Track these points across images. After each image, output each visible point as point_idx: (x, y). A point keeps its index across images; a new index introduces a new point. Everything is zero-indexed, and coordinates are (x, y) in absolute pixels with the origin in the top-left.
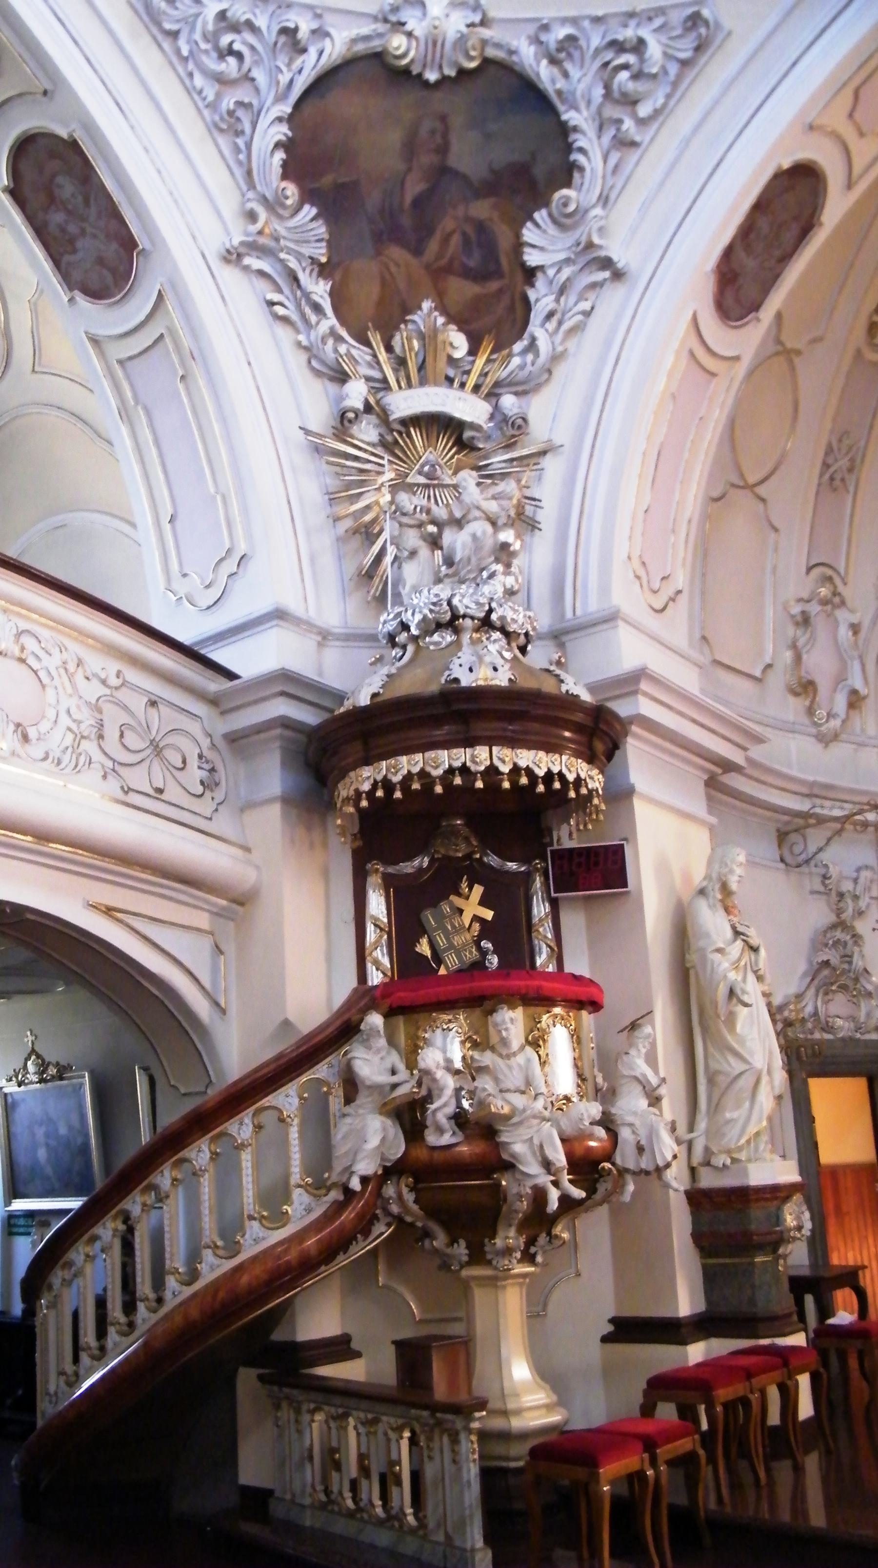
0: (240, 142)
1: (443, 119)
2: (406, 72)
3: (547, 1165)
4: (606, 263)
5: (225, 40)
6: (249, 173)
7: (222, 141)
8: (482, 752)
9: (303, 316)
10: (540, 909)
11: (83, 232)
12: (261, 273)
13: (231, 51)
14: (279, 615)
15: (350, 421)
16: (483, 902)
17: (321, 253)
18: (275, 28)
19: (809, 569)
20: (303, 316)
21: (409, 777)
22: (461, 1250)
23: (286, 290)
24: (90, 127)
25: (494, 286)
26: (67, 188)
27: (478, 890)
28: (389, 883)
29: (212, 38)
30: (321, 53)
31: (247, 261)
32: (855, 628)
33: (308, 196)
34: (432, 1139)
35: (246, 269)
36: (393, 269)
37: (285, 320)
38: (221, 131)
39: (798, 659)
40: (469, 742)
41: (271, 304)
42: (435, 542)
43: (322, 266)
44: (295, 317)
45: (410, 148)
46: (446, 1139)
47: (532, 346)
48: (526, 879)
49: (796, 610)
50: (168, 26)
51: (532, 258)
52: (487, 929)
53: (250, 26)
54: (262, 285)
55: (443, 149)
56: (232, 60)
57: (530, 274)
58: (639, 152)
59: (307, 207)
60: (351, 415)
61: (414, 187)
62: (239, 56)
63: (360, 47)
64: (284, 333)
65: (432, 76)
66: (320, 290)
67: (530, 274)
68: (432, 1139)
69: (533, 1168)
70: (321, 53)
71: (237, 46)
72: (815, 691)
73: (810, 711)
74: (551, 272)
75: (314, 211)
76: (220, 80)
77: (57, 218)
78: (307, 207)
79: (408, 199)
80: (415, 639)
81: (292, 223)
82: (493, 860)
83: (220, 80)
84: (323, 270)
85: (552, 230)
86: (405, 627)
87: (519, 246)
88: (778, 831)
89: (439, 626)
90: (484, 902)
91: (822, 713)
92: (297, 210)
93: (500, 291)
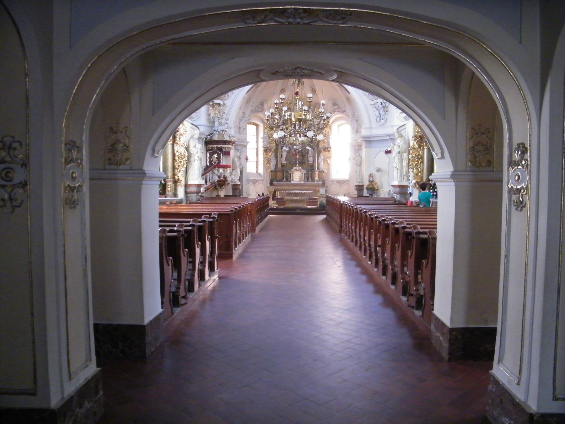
3: (230, 181)
10: (221, 157)
21: (220, 147)
22: (219, 188)
27: (216, 154)
28: (210, 153)
32: (245, 120)
34: (221, 178)
39: (239, 125)
40: (226, 145)
42: (219, 120)
46: (223, 179)
47: (228, 95)
48: (220, 154)
49: (240, 118)
52: (217, 158)
68: (221, 178)
69: (229, 181)
73: (239, 131)
86: (217, 130)
89: (221, 131)
90: (217, 155)
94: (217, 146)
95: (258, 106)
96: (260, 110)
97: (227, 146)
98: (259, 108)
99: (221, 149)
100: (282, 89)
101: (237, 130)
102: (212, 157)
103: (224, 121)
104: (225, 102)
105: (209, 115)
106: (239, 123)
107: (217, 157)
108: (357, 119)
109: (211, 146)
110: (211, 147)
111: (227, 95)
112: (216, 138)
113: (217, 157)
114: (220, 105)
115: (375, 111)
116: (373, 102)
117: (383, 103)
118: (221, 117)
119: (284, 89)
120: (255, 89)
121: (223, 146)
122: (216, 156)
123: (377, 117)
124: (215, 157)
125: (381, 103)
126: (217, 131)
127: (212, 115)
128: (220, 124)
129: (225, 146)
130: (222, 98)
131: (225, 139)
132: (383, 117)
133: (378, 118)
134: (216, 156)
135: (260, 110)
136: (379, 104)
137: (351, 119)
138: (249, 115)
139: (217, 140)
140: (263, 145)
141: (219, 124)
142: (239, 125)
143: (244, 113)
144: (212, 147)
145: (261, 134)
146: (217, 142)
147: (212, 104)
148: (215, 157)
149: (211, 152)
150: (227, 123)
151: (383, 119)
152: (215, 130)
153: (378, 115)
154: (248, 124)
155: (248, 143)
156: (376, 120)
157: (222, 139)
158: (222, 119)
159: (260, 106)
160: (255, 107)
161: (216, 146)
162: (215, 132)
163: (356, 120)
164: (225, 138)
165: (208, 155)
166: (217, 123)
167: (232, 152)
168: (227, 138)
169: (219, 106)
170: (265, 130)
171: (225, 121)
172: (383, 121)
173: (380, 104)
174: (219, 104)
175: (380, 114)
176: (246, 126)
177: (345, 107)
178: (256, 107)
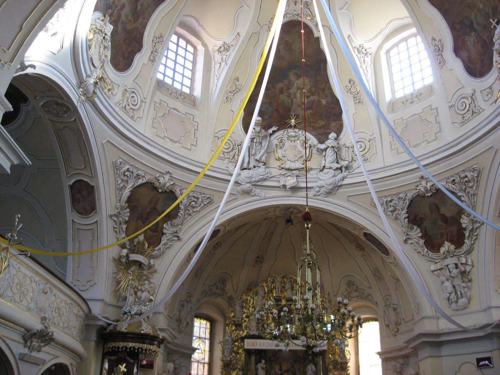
0: (121, 192)
1: (159, 198)
2: (155, 188)
4: (178, 237)
5: (126, 173)
6: (120, 200)
7: (117, 191)
8: (145, 345)
9: (120, 232)
10: (135, 370)
11: (83, 201)
12: (115, 221)
13: (127, 176)
14: (102, 300)
15: (122, 258)
16: (122, 366)
17: (127, 219)
18: (136, 173)
19: (187, 294)
20: (120, 232)
21: (131, 347)
23: (118, 225)
24: (98, 187)
25: (156, 234)
26: (85, 193)
27: (124, 365)
28: (110, 362)
29: (124, 172)
30: (143, 180)
31: (113, 218)
32: (191, 308)
33: (128, 207)
35: (113, 219)
36: (138, 225)
37: (116, 232)
38: (118, 189)
40: (144, 343)
41: (114, 228)
42: (136, 293)
43: (126, 221)
44: (118, 232)
45: (150, 202)
48: (133, 365)
50: (117, 168)
51: (165, 231)
53: (132, 172)
54: (115, 224)
55: (156, 204)
56: (126, 177)
57: (163, 234)
58: (191, 217)
59: (128, 209)
60: (123, 257)
61: (148, 210)
62: (128, 177)
63: (149, 181)
64: (114, 233)
65: (160, 191)
66: (124, 227)
67: (163, 234)
70: (143, 180)
71: (128, 175)
72: (181, 322)
73: (179, 326)
74: (167, 235)
75: (129, 211)
76: (123, 180)
77: (79, 196)
78: (128, 209)
79: (146, 212)
80: (131, 315)
81: (124, 212)
82: (128, 358)
83: (123, 180)
84: (126, 222)
85: (170, 225)
86: (130, 312)
87: (163, 227)
88: (168, 352)
89: (137, 314)
91: (181, 326)
92: (126, 209)
93: (156, 235)
94: (125, 344)
95: (215, 284)
96: (219, 291)
97: (146, 346)
98: (217, 288)
99: (134, 354)
100: (258, 257)
101: (175, 325)
102: (115, 369)
103: (144, 295)
104: (152, 261)
105: (118, 283)
106: (180, 311)
107: (125, 370)
108: (396, 306)
109: (113, 344)
110: (113, 347)
111: (157, 248)
112: (123, 327)
113: (125, 370)
114: (142, 266)
115: (443, 283)
116: (433, 267)
117: (459, 264)
118: (140, 287)
119: (262, 258)
120: (212, 251)
121: (137, 345)
122: (123, 368)
123: (450, 293)
124: (122, 370)
125: (456, 264)
126: (129, 314)
127: (123, 284)
128: (139, 301)
129: (141, 345)
130: (147, 253)
131: (142, 332)
132: (463, 291)
133: (453, 294)
134: (123, 368)
135: (219, 291)
136: (452, 266)
137: (384, 309)
138: (199, 300)
139: (126, 331)
140: (221, 356)
141: (135, 302)
142: (180, 314)
143: (190, 295)
144: (115, 347)
145: (219, 337)
146: (124, 336)
147: (126, 262)
148: (122, 370)
149: (113, 358)
150: (151, 300)
151: (462, 297)
152: (125, 313)
153: (450, 289)
154: (198, 316)
155: (194, 350)
156: (449, 299)
157: (137, 331)
158: (142, 291)
159: (218, 285)
160: (209, 286)
161: (121, 344)
162: (125, 316)
163: (395, 309)
164: (143, 329)
165: (106, 366)
166: (131, 299)
167: (159, 361)
168: (146, 329)
169: (141, 269)
170: (227, 328)
171: (148, 295)
172: (462, 301)
173: (454, 266)
174: (140, 264)
175: (454, 287)
176: (192, 322)
177: (370, 288)
178: (212, 286)
